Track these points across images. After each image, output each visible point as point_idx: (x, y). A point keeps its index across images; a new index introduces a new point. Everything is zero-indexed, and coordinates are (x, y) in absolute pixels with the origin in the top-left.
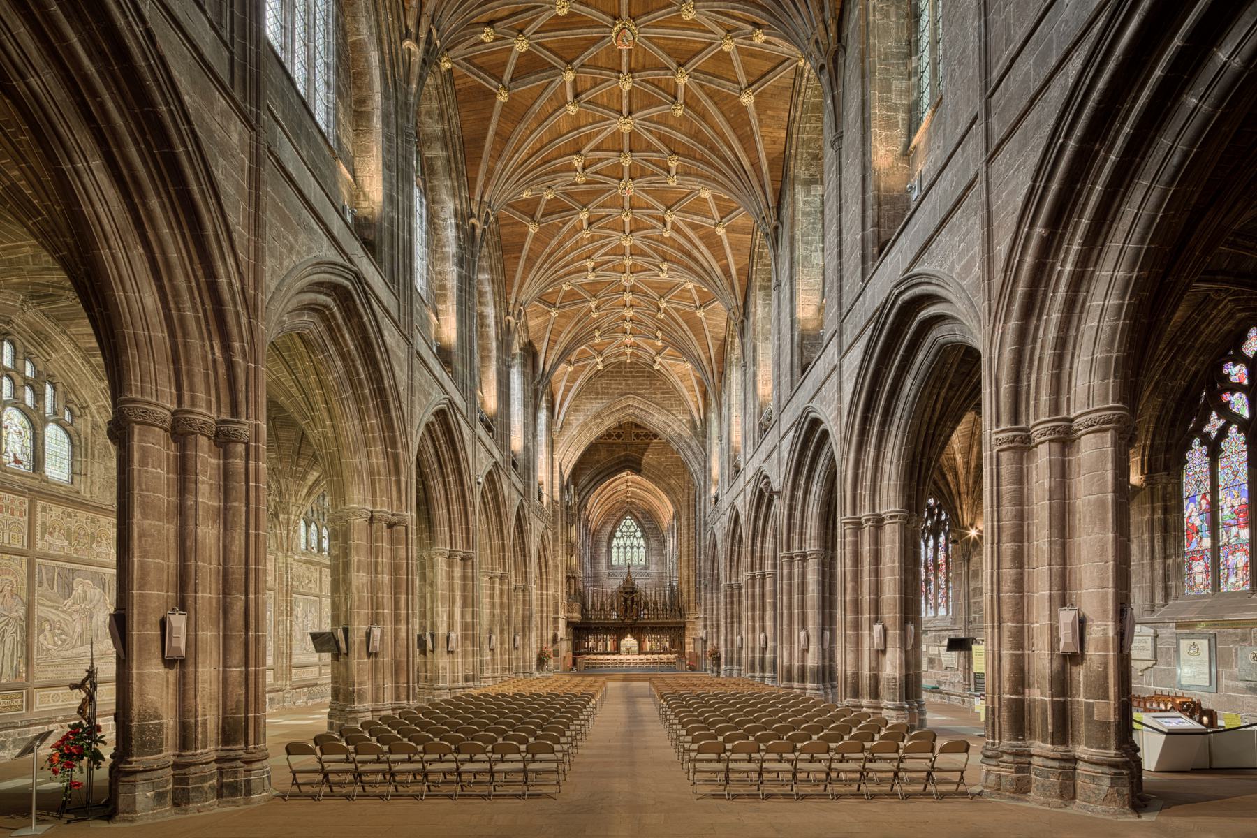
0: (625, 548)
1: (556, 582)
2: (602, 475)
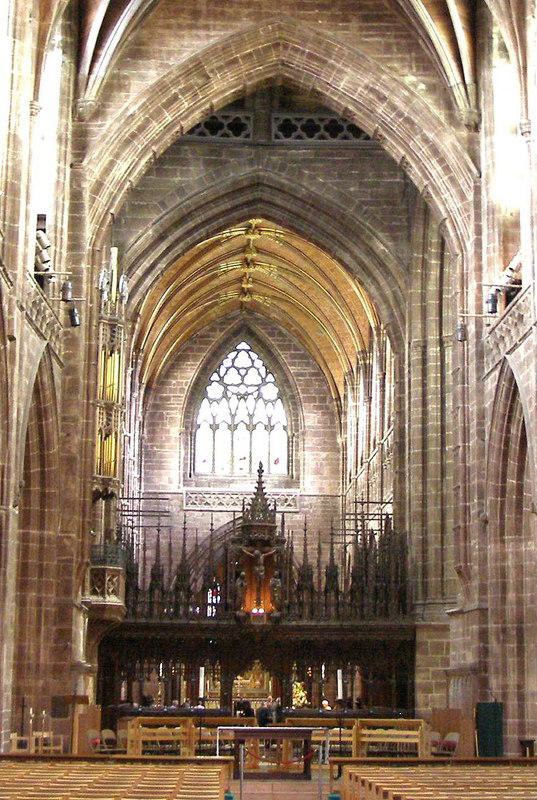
0: (233, 428)
1: (67, 504)
2: (191, 224)
